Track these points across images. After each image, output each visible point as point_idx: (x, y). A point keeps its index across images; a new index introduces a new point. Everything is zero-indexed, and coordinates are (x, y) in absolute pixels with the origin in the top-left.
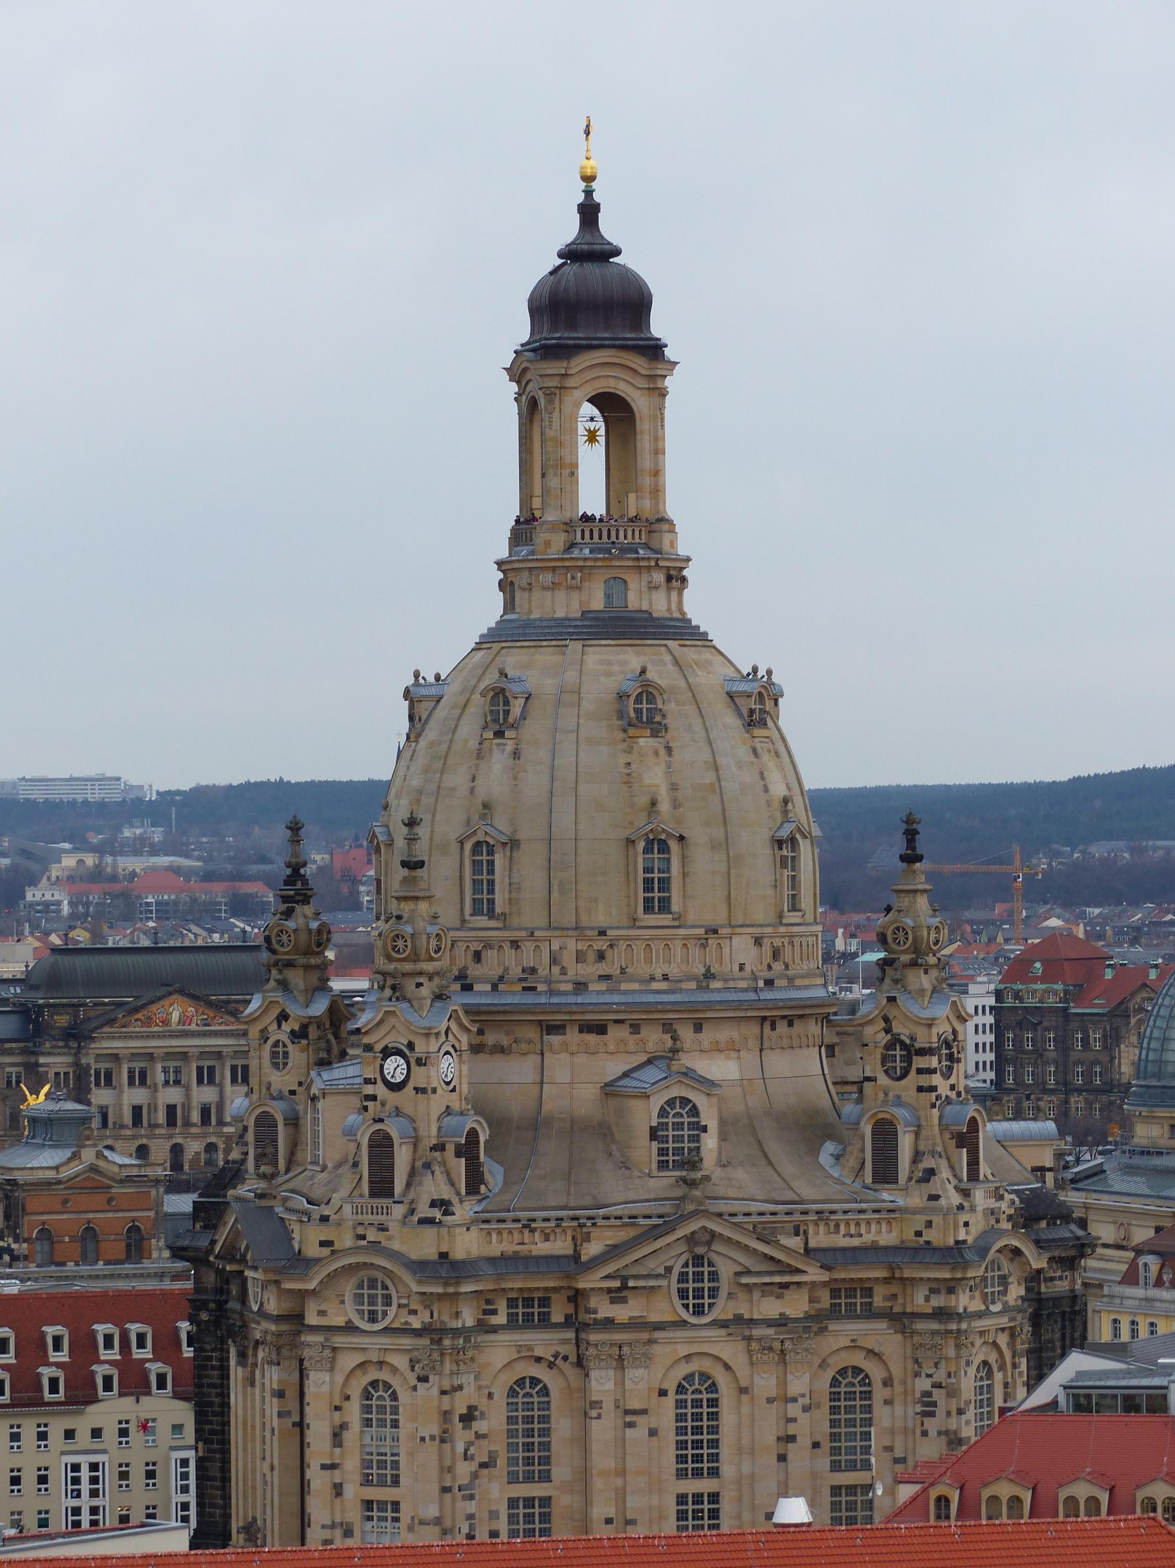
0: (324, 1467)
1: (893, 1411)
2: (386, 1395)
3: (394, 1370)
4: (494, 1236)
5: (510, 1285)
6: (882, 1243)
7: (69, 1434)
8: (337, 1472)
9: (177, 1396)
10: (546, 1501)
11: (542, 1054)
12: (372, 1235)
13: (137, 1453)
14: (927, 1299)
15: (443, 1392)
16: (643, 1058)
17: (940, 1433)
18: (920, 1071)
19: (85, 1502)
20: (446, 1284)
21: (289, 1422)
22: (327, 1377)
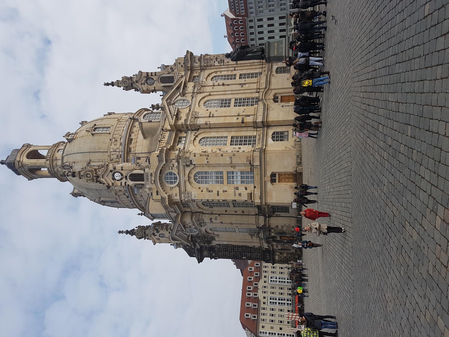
0: (218, 195)
1: (223, 71)
3: (190, 173)
5: (172, 143)
7: (264, 303)
10: (232, 137)
14: (197, 63)
15: (195, 156)
16: (140, 131)
18: (152, 75)
19: (277, 301)
21: (218, 217)
22: (193, 193)
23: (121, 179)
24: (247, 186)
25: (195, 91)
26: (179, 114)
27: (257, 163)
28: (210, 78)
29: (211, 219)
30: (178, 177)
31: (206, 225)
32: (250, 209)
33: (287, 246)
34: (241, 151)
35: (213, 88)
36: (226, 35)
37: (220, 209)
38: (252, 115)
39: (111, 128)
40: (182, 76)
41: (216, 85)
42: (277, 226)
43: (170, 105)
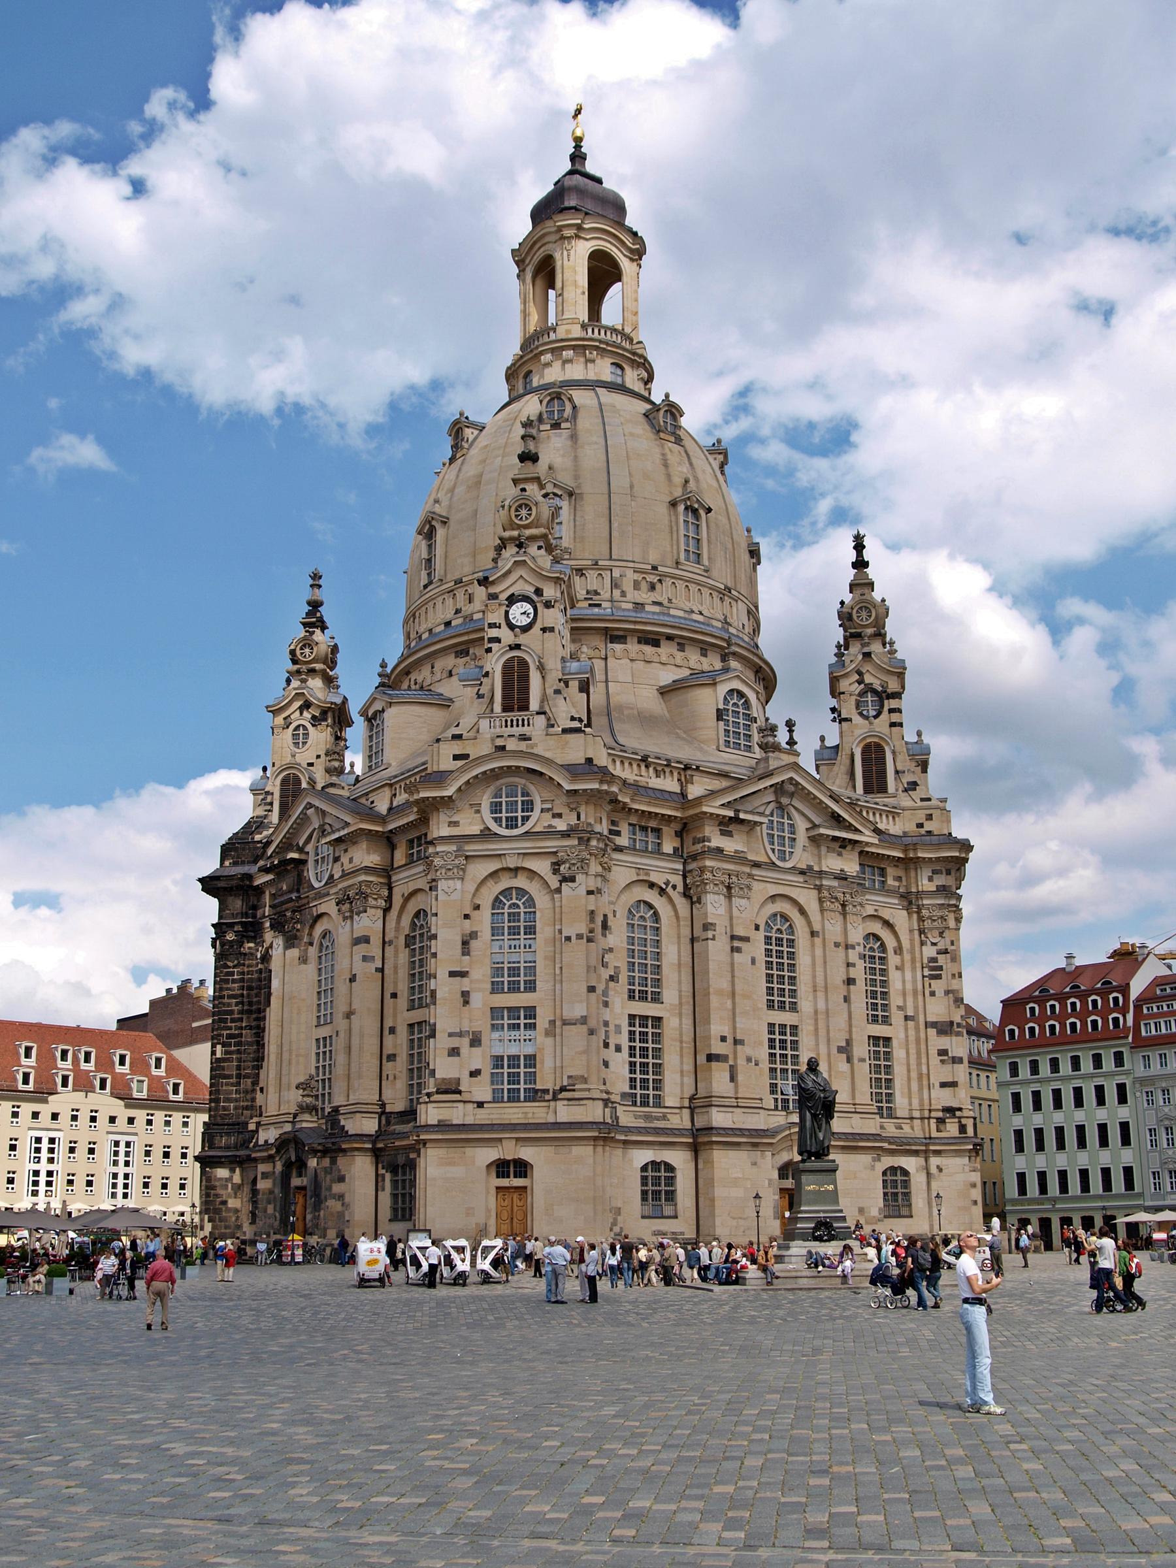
0: (452, 974)
2: (520, 903)
3: (532, 874)
4: (618, 763)
6: (891, 832)
7: (35, 1115)
8: (465, 979)
9: (112, 1095)
11: (606, 659)
12: (512, 745)
13: (83, 1134)
14: (930, 879)
15: (590, 893)
17: (947, 992)
18: (891, 711)
19: (44, 1167)
20: (601, 782)
21: (372, 967)
22: (458, 884)
23: (512, 627)
24: (485, 1076)
25: (825, 882)
26: (745, 828)
27: (564, 1112)
28: (876, 928)
29: (366, 940)
30: (515, 832)
31: (345, 919)
32: (401, 1085)
33: (270, 1209)
34: (610, 1054)
35: (837, 945)
36: (1078, 962)
37: (403, 974)
38: (736, 1092)
39: (698, 569)
40: (877, 831)
41: (847, 956)
42: (341, 1179)
43: (775, 792)
